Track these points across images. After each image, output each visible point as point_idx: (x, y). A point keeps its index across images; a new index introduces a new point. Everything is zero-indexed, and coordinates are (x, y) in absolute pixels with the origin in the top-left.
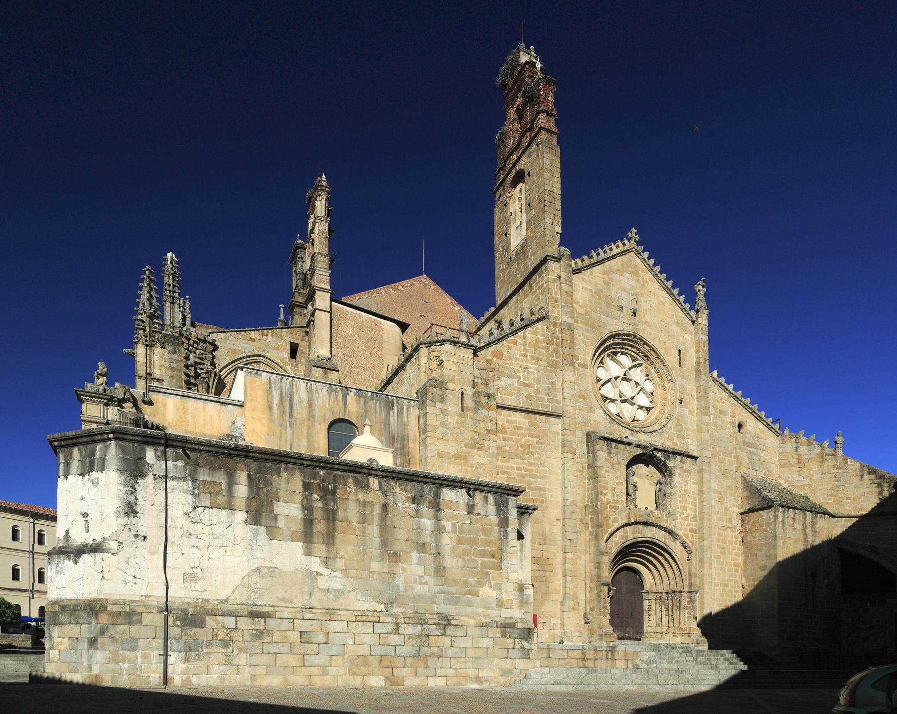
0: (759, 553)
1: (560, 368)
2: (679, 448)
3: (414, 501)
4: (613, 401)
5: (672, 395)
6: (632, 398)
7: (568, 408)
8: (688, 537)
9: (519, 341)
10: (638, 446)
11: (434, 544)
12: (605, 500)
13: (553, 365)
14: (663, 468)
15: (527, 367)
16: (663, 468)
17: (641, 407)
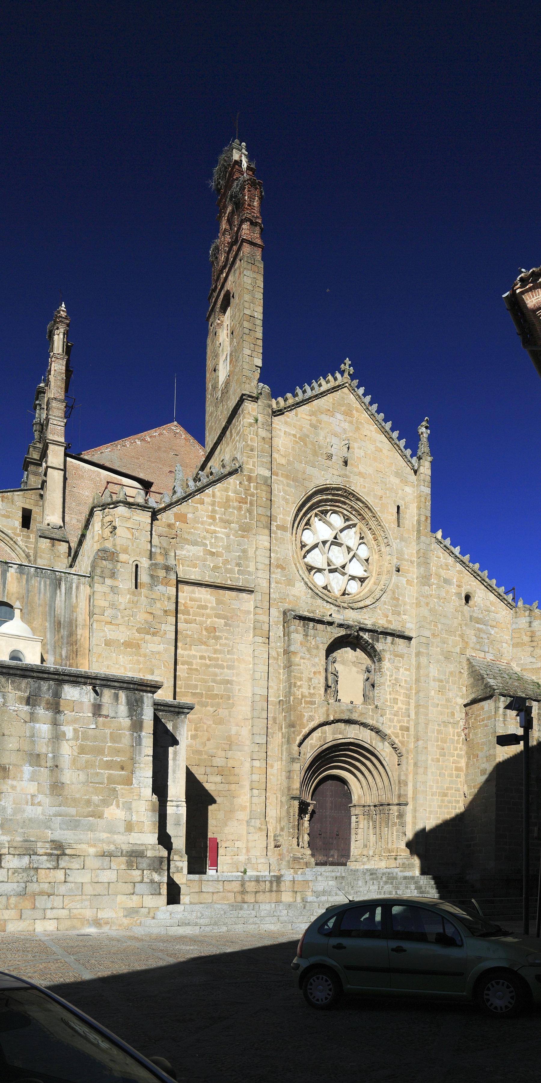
0: (480, 754)
1: (254, 531)
2: (394, 626)
3: (28, 701)
4: (320, 570)
6: (343, 567)
7: (260, 581)
8: (397, 737)
9: (207, 500)
11: (50, 755)
12: (298, 693)
13: (245, 529)
14: (371, 653)
15: (215, 532)
16: (371, 653)
17: (353, 578)
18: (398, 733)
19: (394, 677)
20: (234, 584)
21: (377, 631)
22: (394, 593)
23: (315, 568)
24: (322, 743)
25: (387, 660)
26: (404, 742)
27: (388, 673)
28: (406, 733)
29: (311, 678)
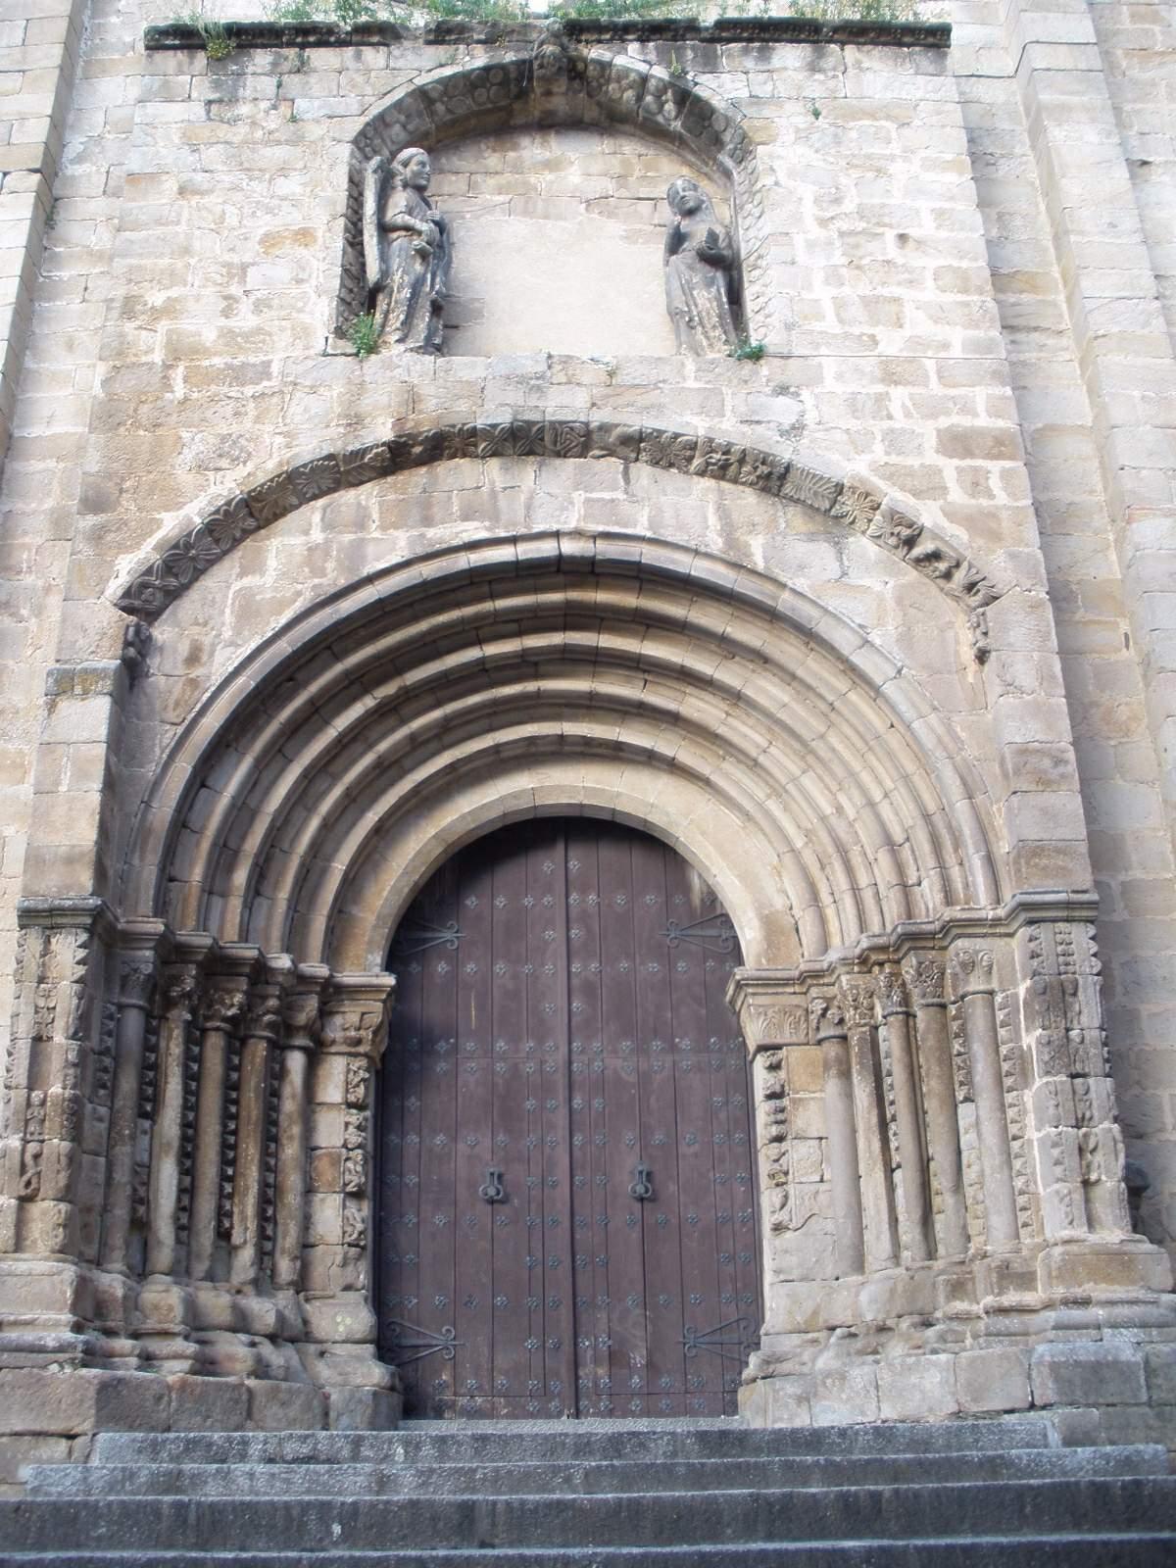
10: (441, 34)
19: (849, 206)
21: (690, 28)
24: (334, 578)
26: (992, 515)
27: (808, 191)
28: (995, 467)
29: (244, 268)
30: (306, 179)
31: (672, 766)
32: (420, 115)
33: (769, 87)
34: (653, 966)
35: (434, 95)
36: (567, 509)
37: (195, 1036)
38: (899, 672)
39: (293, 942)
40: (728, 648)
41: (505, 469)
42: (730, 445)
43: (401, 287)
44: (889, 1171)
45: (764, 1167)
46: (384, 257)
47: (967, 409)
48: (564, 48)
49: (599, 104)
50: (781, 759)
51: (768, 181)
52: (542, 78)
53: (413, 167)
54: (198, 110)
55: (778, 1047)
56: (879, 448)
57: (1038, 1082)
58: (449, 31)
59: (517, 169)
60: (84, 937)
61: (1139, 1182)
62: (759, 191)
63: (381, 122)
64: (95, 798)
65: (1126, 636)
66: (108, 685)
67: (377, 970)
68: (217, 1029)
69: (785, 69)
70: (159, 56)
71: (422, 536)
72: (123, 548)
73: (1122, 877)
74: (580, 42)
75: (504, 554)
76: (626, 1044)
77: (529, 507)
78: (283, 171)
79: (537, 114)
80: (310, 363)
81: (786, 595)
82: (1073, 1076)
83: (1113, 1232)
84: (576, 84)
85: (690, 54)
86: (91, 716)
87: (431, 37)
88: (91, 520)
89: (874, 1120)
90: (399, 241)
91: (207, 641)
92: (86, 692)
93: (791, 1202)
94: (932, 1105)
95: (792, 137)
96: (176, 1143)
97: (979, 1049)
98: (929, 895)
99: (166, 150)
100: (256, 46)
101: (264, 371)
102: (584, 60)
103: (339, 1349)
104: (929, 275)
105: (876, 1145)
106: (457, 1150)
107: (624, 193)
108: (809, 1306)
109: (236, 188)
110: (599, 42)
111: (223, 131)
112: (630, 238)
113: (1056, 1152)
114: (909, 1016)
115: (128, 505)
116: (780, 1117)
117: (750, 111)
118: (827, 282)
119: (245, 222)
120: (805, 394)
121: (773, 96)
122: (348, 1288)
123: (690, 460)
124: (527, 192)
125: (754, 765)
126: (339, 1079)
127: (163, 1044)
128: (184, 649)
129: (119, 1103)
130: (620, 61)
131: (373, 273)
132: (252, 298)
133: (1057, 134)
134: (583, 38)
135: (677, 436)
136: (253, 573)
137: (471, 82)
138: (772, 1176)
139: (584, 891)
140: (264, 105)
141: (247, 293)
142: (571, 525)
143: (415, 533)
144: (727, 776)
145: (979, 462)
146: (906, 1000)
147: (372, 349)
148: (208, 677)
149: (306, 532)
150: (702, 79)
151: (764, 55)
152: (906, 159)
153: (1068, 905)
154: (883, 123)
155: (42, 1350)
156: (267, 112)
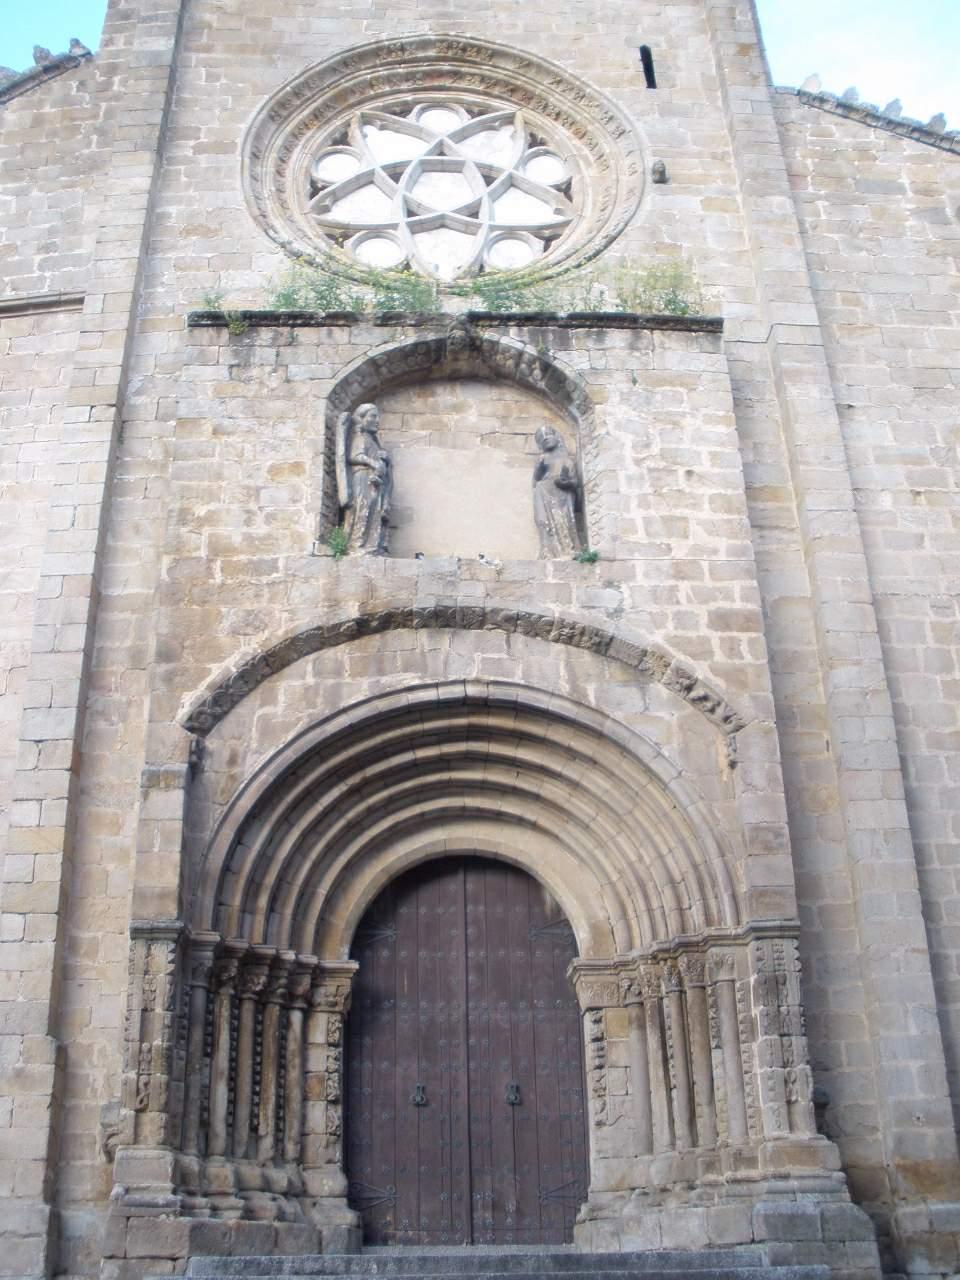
5: (628, 166)
10: (387, 320)
14: (557, 390)
18: (706, 641)
19: (655, 449)
20: (24, 294)
21: (552, 318)
22: (653, 233)
23: (358, 229)
25: (615, 398)
26: (741, 670)
27: (628, 439)
28: (744, 636)
29: (258, 490)
30: (296, 426)
31: (534, 826)
32: (371, 375)
33: (603, 362)
34: (520, 953)
35: (380, 362)
36: (469, 664)
37: (237, 1003)
38: (680, 773)
39: (295, 942)
40: (572, 754)
41: (431, 637)
42: (575, 623)
43: (362, 507)
44: (669, 1089)
45: (591, 1085)
46: (350, 485)
47: (729, 597)
48: (466, 330)
49: (490, 367)
50: (603, 824)
51: (603, 431)
52: (454, 352)
53: (368, 418)
54: (224, 371)
55: (599, 1009)
56: (670, 625)
57: (761, 1038)
58: (391, 318)
59: (434, 410)
60: (172, 946)
61: (823, 1100)
62: (596, 438)
63: (345, 383)
64: (177, 857)
65: (827, 742)
66: (182, 782)
67: (346, 957)
68: (250, 999)
69: (614, 348)
70: (197, 332)
71: (378, 681)
72: (186, 688)
73: (821, 903)
74: (477, 326)
75: (429, 695)
76: (503, 1004)
77: (446, 663)
78: (282, 418)
79: (448, 371)
80: (304, 561)
81: (608, 723)
82: (782, 1035)
83: (805, 1133)
84: (475, 354)
85: (551, 337)
86: (171, 802)
87: (379, 322)
88: (163, 668)
89: (660, 1057)
90: (359, 472)
91: (241, 750)
92: (168, 787)
93: (608, 1107)
94: (696, 1051)
95: (618, 399)
96: (226, 1073)
97: (725, 1017)
98: (696, 916)
99: (204, 401)
100: (262, 326)
101: (273, 566)
102: (482, 341)
103: (326, 1202)
104: (706, 500)
105: (661, 1073)
106: (397, 1072)
107: (506, 429)
108: (618, 1175)
109: (250, 431)
110: (491, 326)
111: (241, 389)
112: (510, 463)
113: (770, 1083)
114: (682, 992)
115: (188, 659)
116: (601, 1053)
117: (590, 379)
118: (639, 506)
119: (258, 457)
120: (624, 587)
121: (605, 369)
122: (330, 1162)
123: (549, 632)
124: (440, 428)
125: (586, 828)
126: (324, 1028)
127: (217, 1010)
128: (226, 755)
129: (192, 1049)
130: (504, 340)
131: (343, 497)
132: (264, 513)
133: (793, 391)
134: (481, 323)
135: (541, 617)
136: (269, 704)
137: (405, 353)
138: (596, 1091)
139: (476, 902)
140: (268, 369)
141: (260, 508)
142: (474, 675)
143: (373, 679)
144: (569, 833)
145: (735, 634)
146: (680, 982)
147: (344, 552)
148: (242, 773)
149: (303, 678)
150: (559, 355)
151: (600, 338)
152: (693, 416)
153: (781, 928)
154: (681, 389)
155: (156, 1206)
156: (270, 374)
